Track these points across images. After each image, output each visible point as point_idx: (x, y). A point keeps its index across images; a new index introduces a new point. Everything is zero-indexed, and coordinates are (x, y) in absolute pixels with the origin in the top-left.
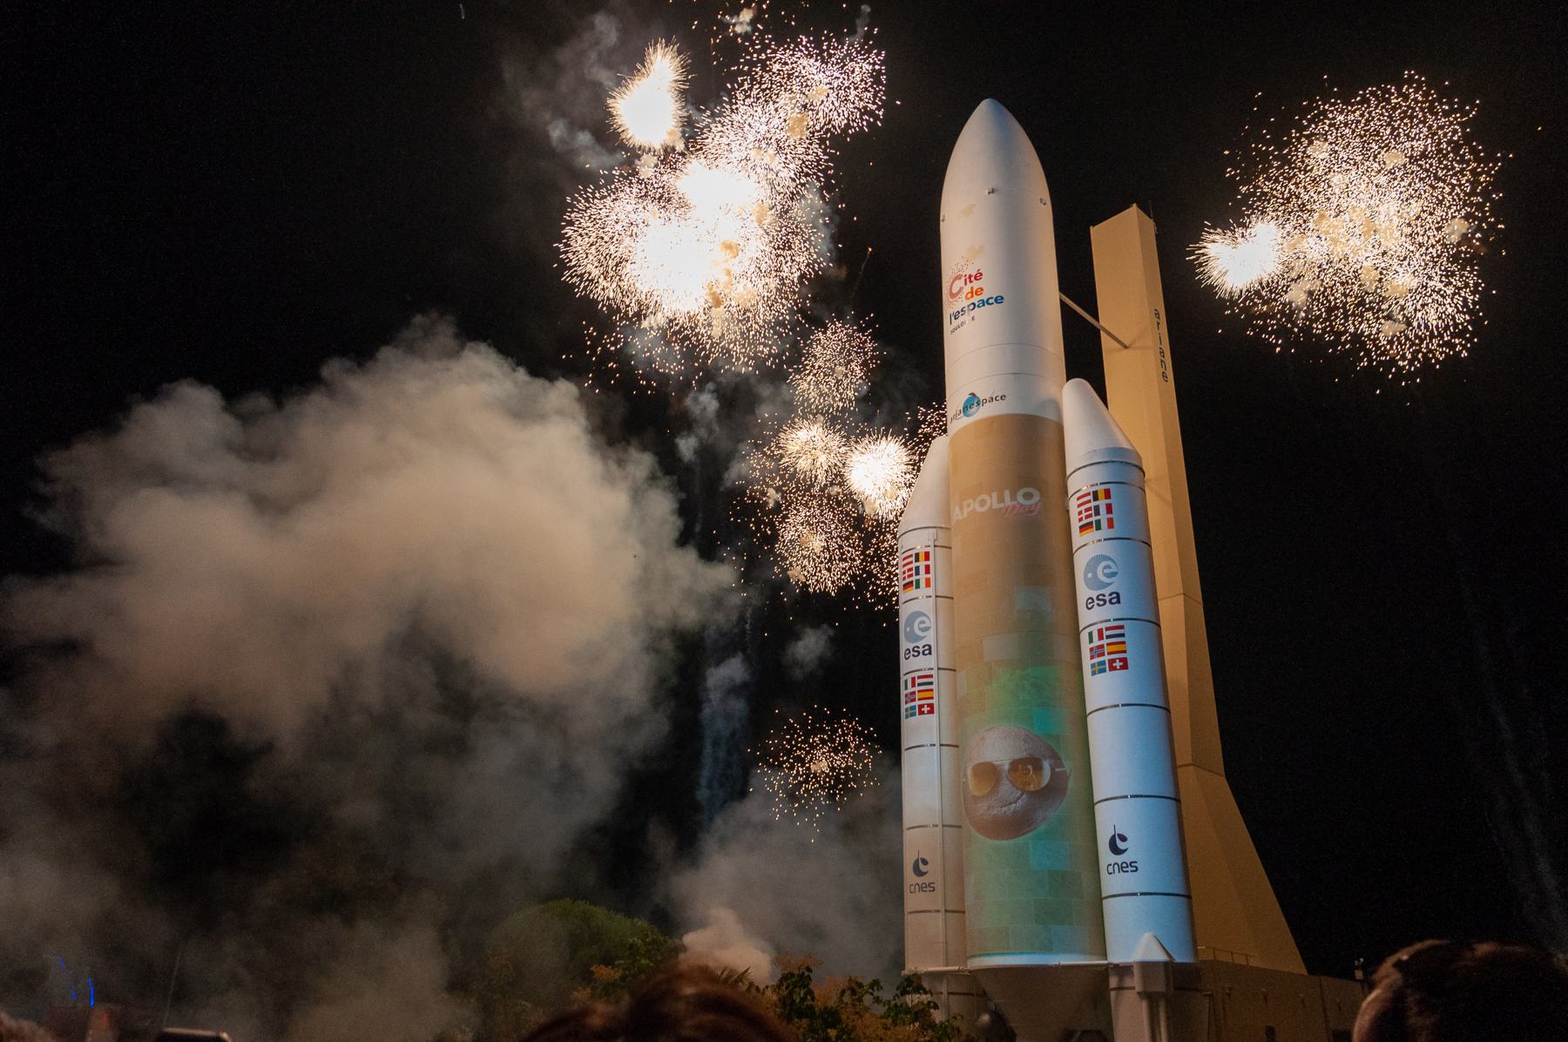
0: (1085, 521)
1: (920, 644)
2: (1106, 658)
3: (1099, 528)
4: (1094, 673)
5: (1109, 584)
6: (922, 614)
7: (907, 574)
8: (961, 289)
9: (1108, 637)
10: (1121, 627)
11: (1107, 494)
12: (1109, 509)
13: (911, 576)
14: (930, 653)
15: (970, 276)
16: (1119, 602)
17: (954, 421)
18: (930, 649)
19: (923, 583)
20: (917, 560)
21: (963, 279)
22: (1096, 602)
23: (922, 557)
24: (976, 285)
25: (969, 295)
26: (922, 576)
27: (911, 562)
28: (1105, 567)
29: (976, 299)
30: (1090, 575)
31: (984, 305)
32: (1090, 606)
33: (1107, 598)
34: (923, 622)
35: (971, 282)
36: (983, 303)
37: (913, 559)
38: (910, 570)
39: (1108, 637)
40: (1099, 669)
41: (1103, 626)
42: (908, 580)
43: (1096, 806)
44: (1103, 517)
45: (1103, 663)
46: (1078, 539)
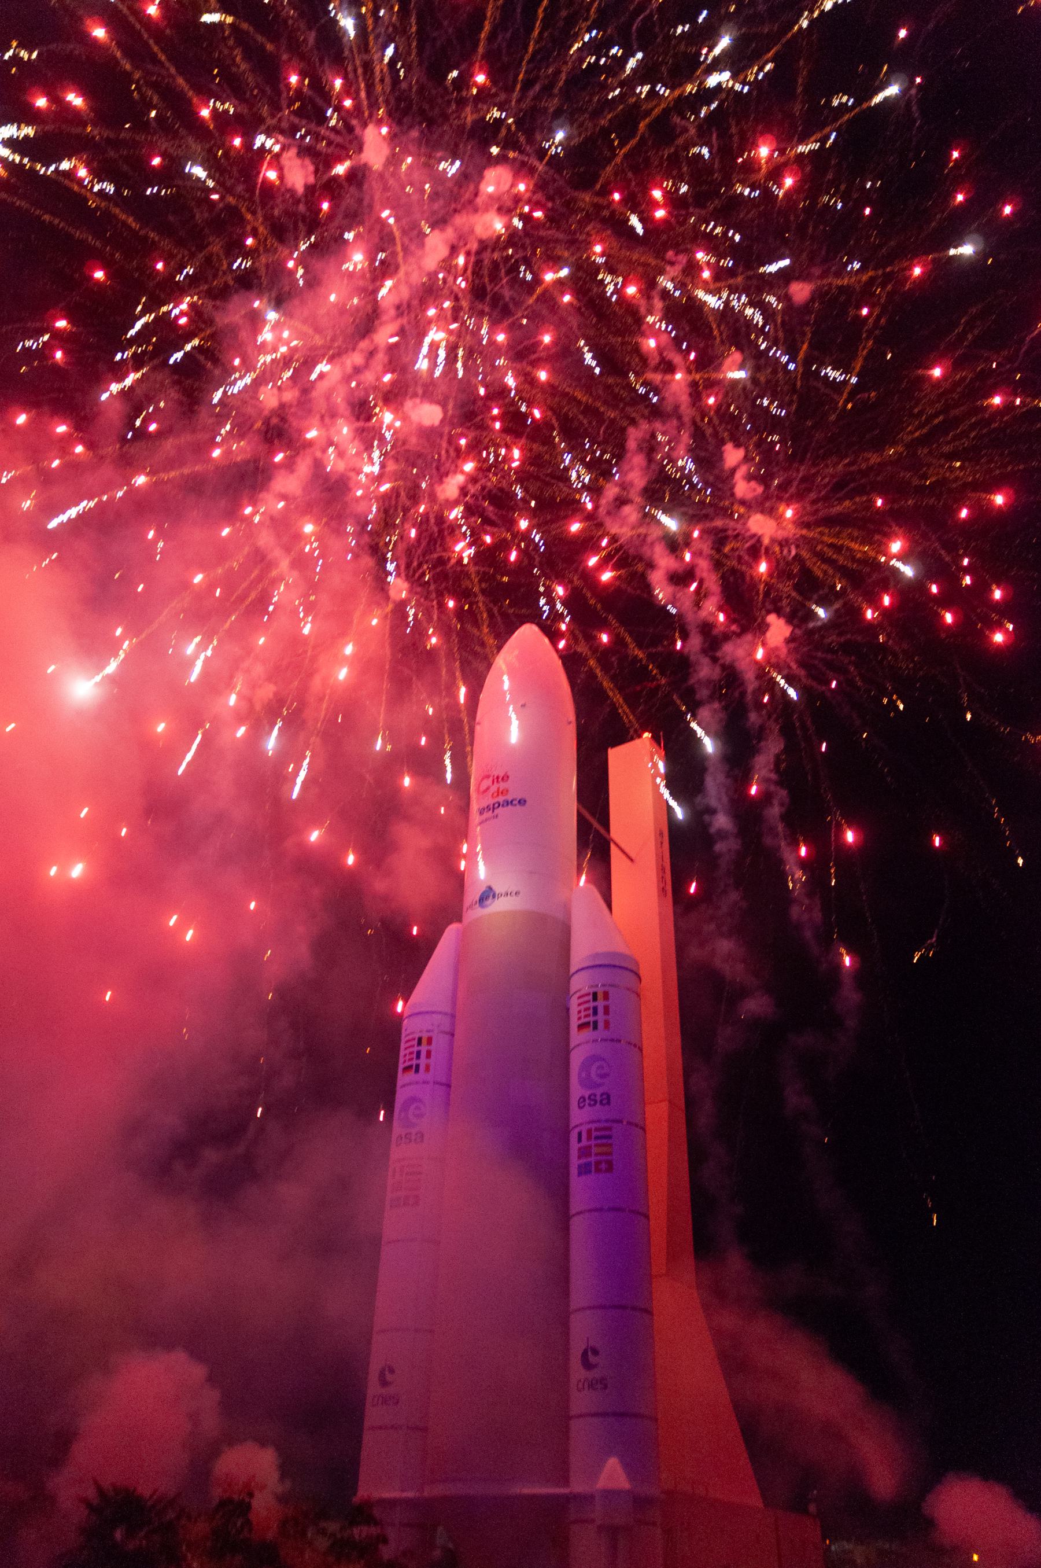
0: (583, 1020)
1: (414, 1131)
2: (593, 1159)
3: (595, 1028)
4: (580, 1174)
5: (599, 1085)
6: (420, 1101)
7: (408, 1057)
8: (488, 788)
9: (597, 1138)
10: (610, 1129)
11: (606, 996)
12: (607, 1011)
13: (410, 1060)
14: (422, 1141)
15: (498, 778)
16: (609, 1103)
17: (470, 911)
18: (422, 1136)
19: (422, 1068)
20: (420, 1042)
21: (491, 779)
22: (587, 1101)
23: (424, 1041)
24: (502, 785)
25: (496, 794)
26: (423, 1061)
27: (413, 1046)
28: (598, 1068)
29: (501, 799)
30: (584, 1075)
31: (508, 804)
32: (582, 1105)
33: (598, 1098)
34: (417, 1108)
35: (498, 781)
36: (508, 803)
37: (416, 1042)
38: (411, 1053)
39: (597, 1138)
40: (584, 1170)
41: (593, 1126)
42: (407, 1064)
43: (572, 1316)
44: (601, 1017)
45: (589, 1164)
46: (576, 1037)
